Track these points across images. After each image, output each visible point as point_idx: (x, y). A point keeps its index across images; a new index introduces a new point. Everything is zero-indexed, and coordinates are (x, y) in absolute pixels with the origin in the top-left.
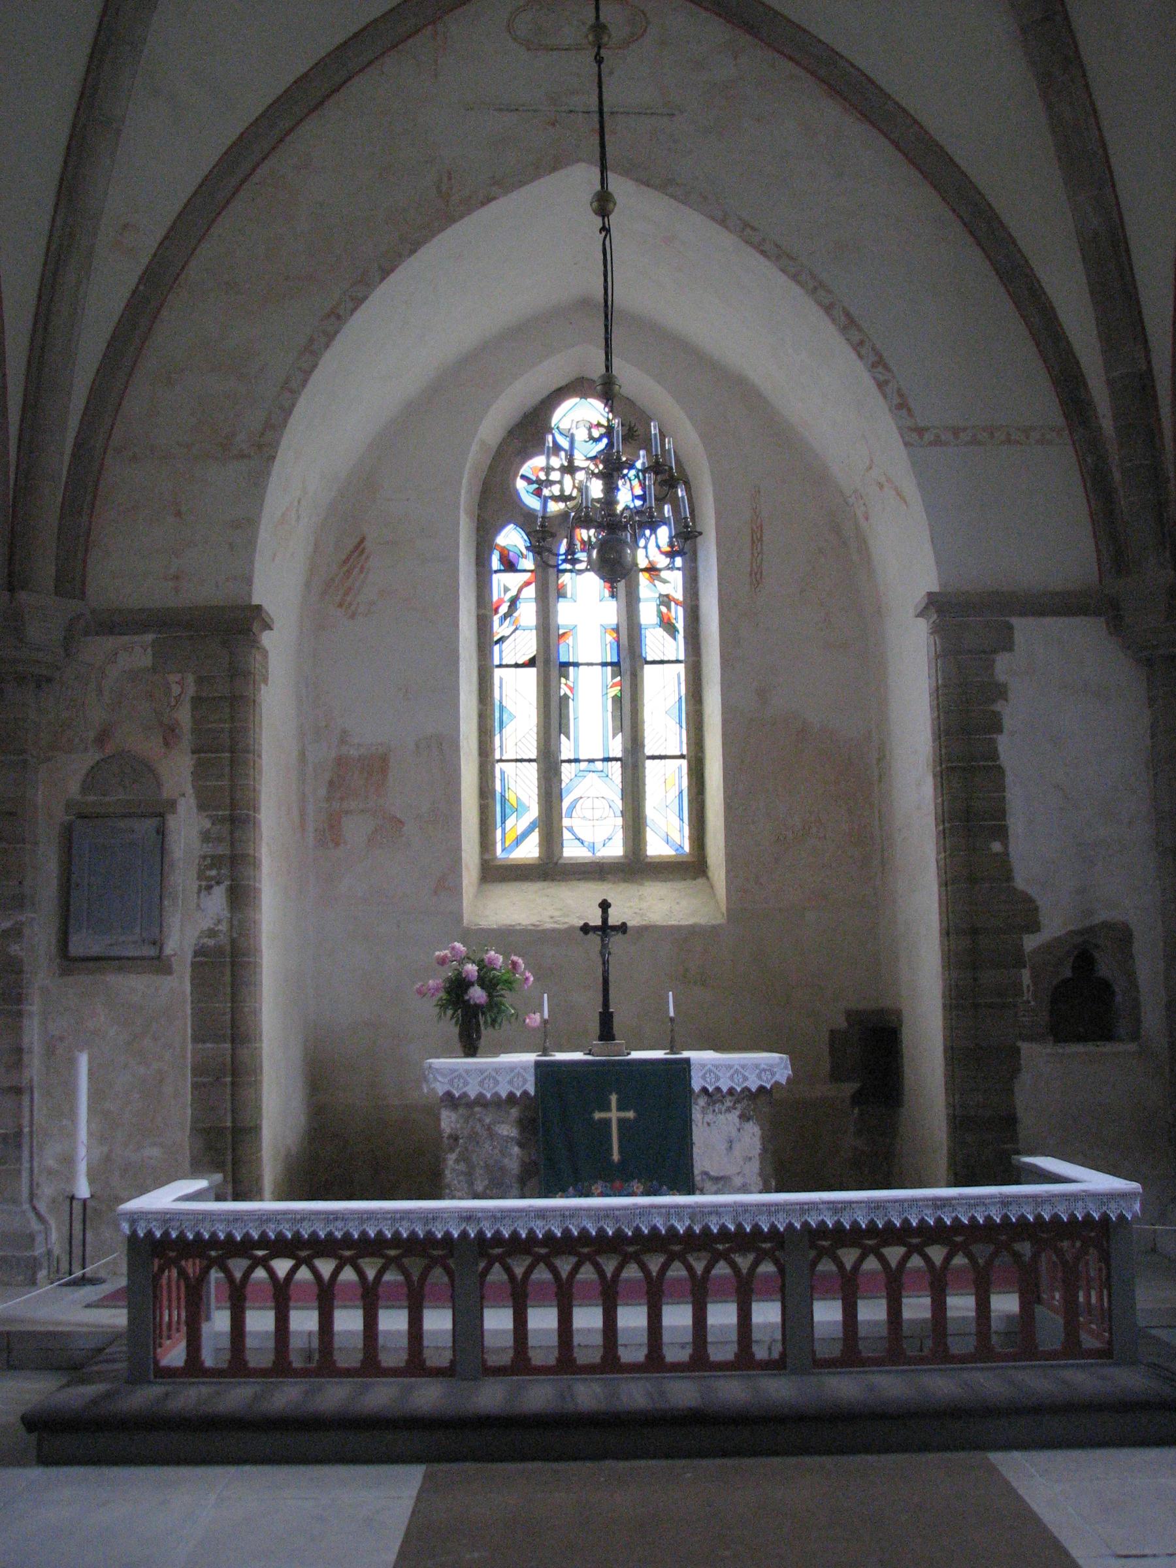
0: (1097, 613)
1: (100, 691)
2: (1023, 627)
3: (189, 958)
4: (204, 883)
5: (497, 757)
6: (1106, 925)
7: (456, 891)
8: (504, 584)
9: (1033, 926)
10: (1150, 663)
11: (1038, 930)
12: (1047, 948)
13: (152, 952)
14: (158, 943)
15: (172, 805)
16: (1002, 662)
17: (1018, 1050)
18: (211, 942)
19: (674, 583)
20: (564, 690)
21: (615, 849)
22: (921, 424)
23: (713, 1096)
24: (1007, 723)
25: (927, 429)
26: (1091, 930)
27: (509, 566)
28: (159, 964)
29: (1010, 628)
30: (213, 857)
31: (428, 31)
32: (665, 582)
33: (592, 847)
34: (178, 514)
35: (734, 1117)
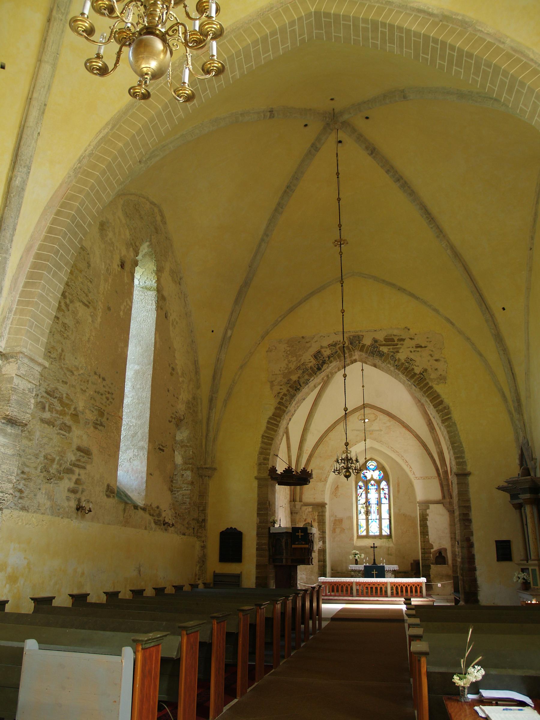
1: (305, 514)
2: (431, 506)
6: (443, 548)
7: (353, 540)
8: (360, 491)
9: (433, 548)
10: (448, 511)
12: (434, 551)
16: (428, 511)
18: (320, 548)
19: (386, 491)
21: (378, 534)
23: (388, 571)
24: (429, 519)
26: (441, 549)
27: (361, 488)
29: (429, 506)
34: (315, 489)
35: (391, 574)
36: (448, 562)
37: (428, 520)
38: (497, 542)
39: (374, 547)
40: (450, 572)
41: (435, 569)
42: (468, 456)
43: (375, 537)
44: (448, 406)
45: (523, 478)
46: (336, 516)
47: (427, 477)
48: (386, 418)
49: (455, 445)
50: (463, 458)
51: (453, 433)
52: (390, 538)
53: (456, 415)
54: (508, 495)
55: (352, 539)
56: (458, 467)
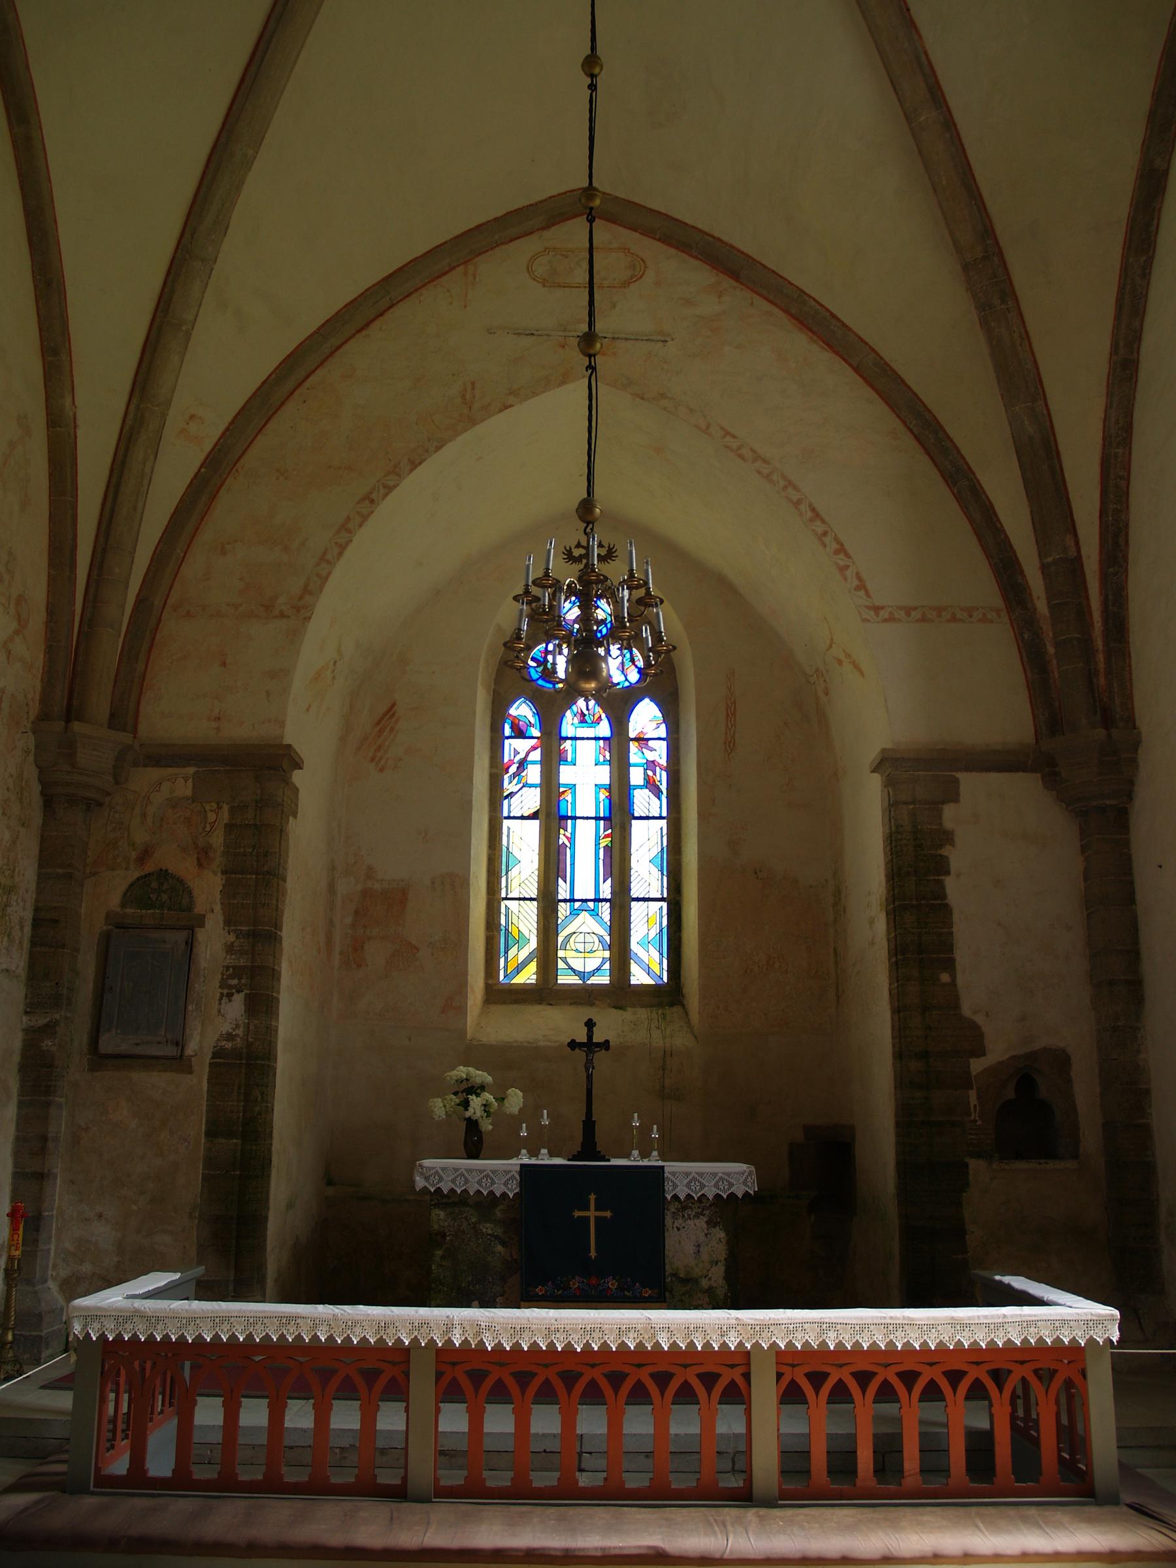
0: (1033, 770)
1: (144, 815)
2: (968, 782)
3: (208, 1059)
4: (225, 991)
5: (503, 895)
7: (462, 1010)
8: (515, 748)
9: (980, 1052)
11: (984, 1055)
13: (171, 1051)
14: (180, 1044)
15: (201, 921)
16: (949, 813)
17: (967, 1165)
18: (229, 1045)
19: (659, 752)
20: (562, 840)
21: (604, 979)
22: (878, 603)
24: (954, 865)
25: (883, 608)
27: (519, 733)
28: (180, 1063)
29: (957, 781)
30: (234, 968)
31: (461, 269)
32: (652, 750)
33: (582, 975)
34: (224, 664)
37: (952, 872)
39: (590, 1046)
43: (585, 995)
46: (370, 873)
47: (939, 610)
48: (698, 275)
52: (672, 1005)
55: (455, 1002)
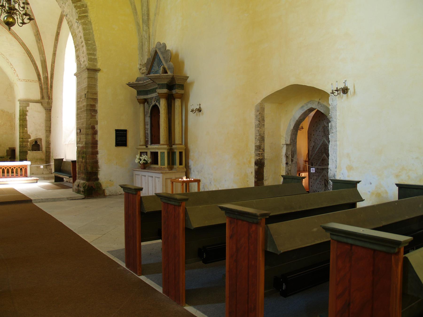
0: (40, 103)
2: (31, 104)
9: (30, 138)
10: (45, 109)
11: (30, 138)
12: (31, 141)
16: (28, 108)
17: (27, 152)
22: (20, 79)
24: (28, 115)
25: (20, 79)
26: (37, 139)
36: (42, 149)
37: (28, 116)
38: (117, 131)
40: (44, 157)
41: (30, 154)
42: (99, 54)
44: (86, 5)
45: (163, 74)
47: (28, 80)
49: (89, 42)
50: (94, 55)
51: (88, 31)
53: (92, 15)
54: (135, 91)
56: (89, 62)
